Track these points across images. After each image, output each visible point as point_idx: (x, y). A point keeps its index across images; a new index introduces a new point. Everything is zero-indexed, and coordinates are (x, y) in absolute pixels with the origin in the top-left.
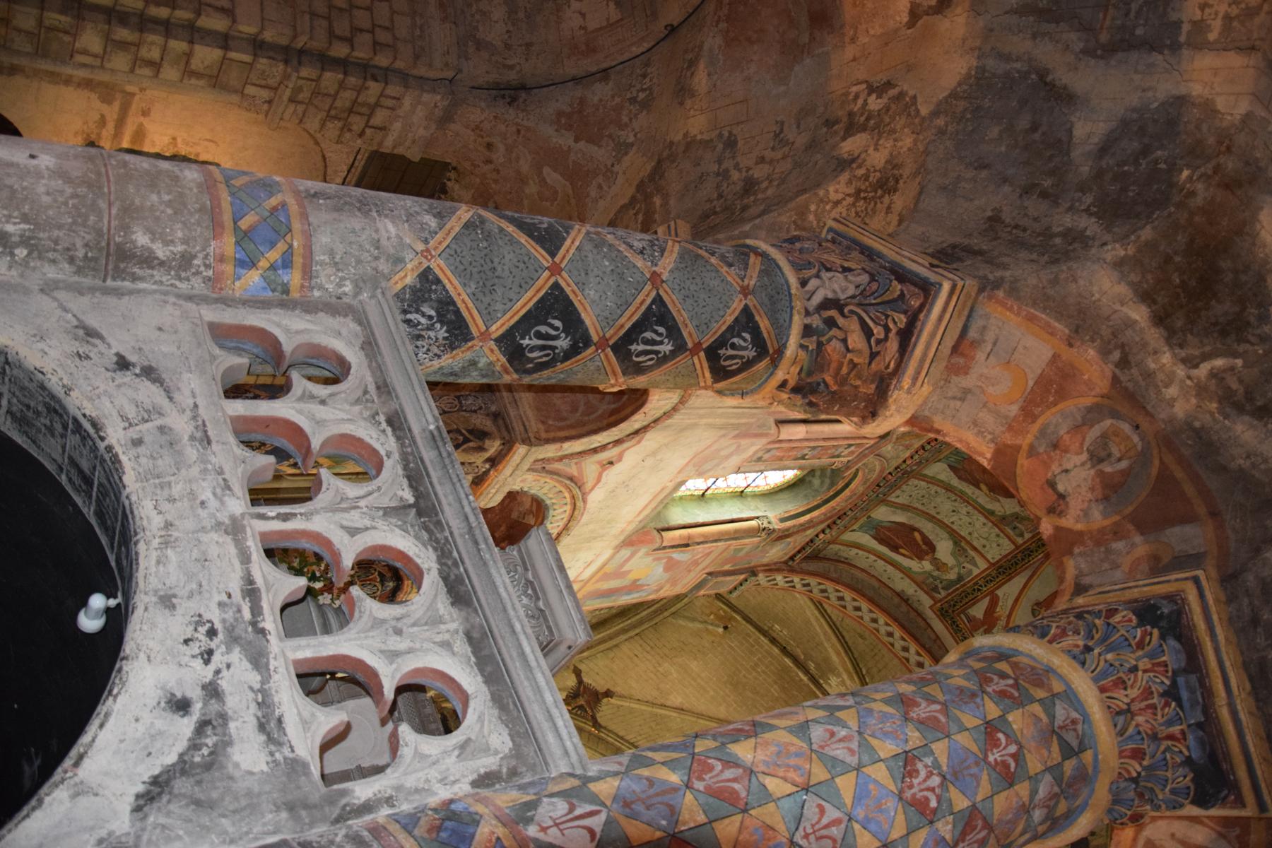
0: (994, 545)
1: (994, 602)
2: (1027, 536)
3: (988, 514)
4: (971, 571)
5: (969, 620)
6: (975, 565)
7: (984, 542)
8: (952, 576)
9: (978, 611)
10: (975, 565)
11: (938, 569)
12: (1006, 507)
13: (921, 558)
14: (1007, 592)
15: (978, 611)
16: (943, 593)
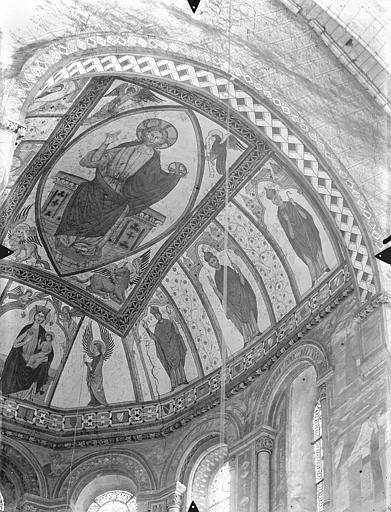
0: (232, 219)
1: (220, 167)
2: (208, 229)
3: (240, 251)
4: (247, 191)
5: (242, 147)
6: (245, 198)
7: (241, 223)
8: (262, 185)
9: (233, 155)
10: (245, 198)
11: (274, 191)
12: (226, 258)
13: (289, 203)
14: (210, 179)
15: (233, 155)
16: (267, 165)
